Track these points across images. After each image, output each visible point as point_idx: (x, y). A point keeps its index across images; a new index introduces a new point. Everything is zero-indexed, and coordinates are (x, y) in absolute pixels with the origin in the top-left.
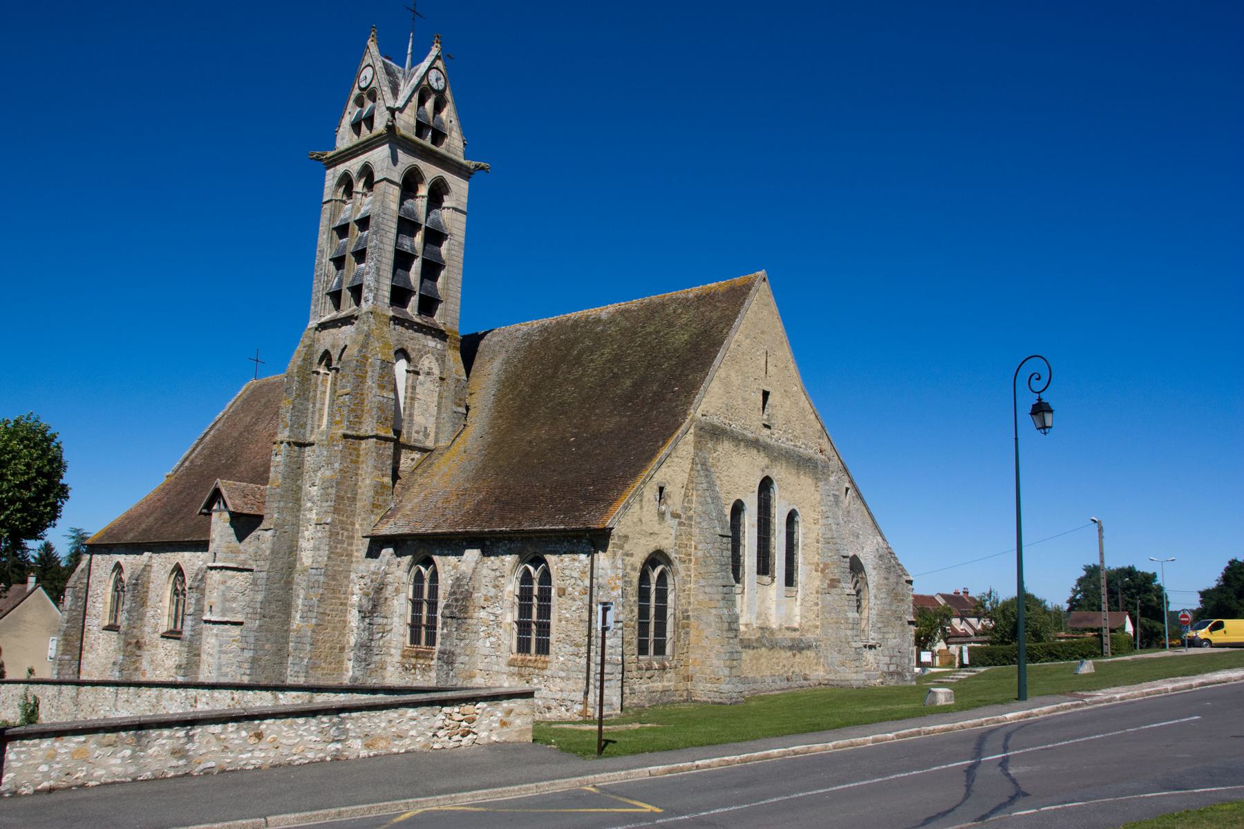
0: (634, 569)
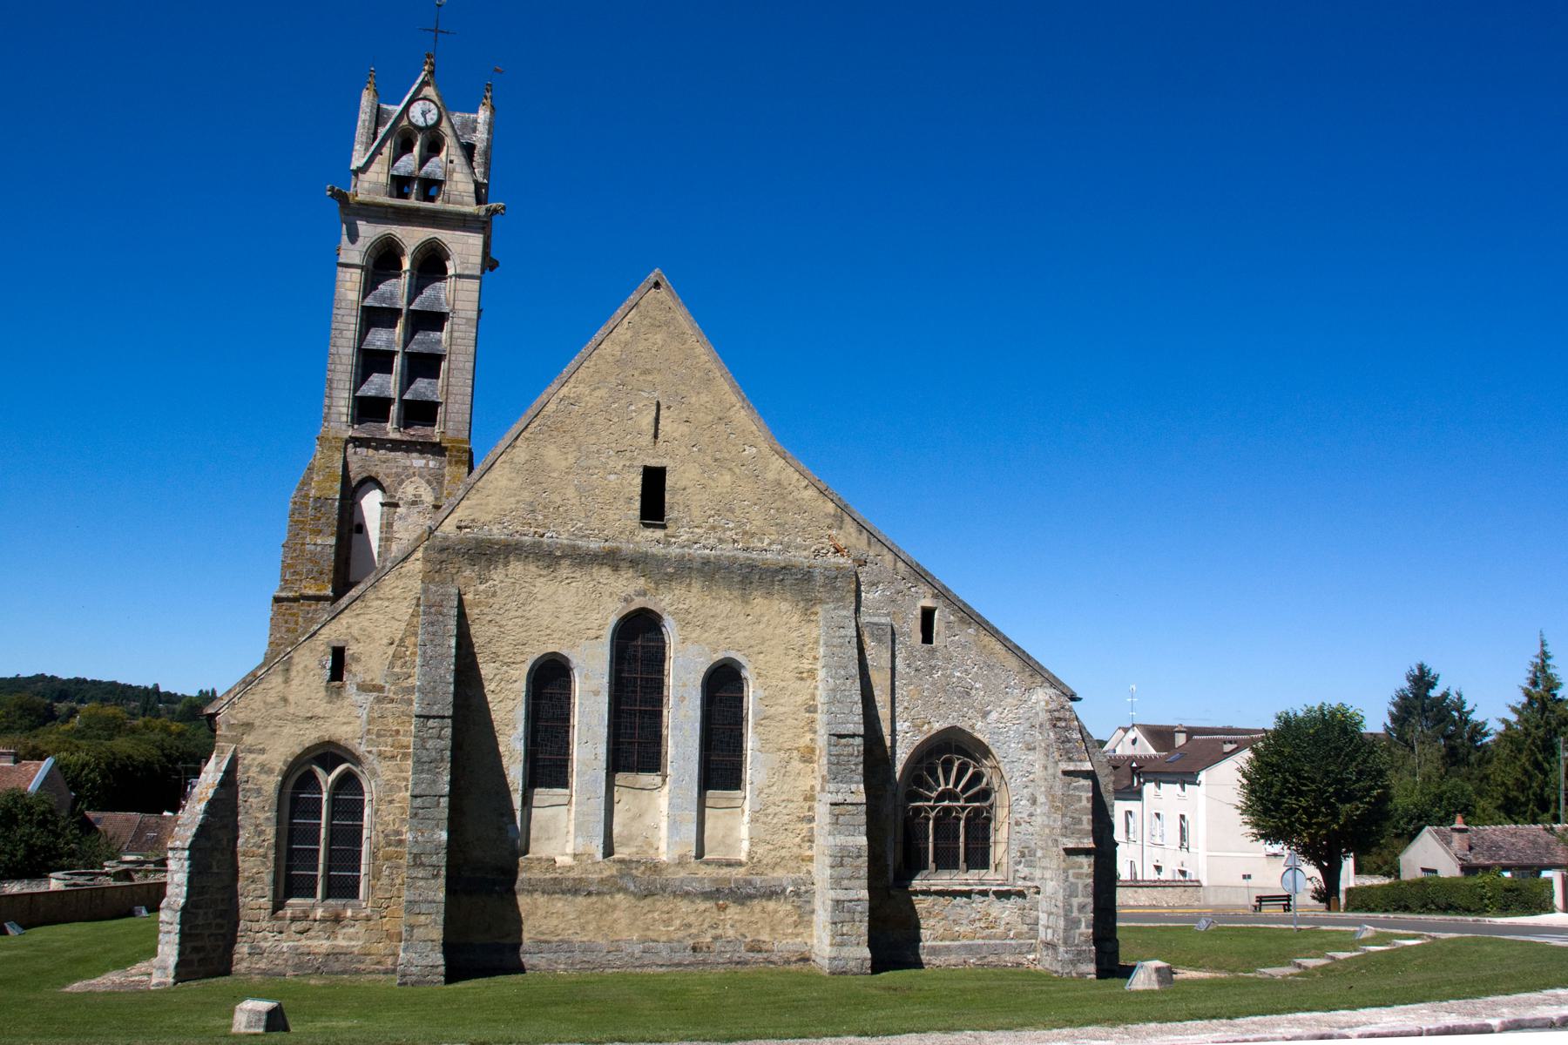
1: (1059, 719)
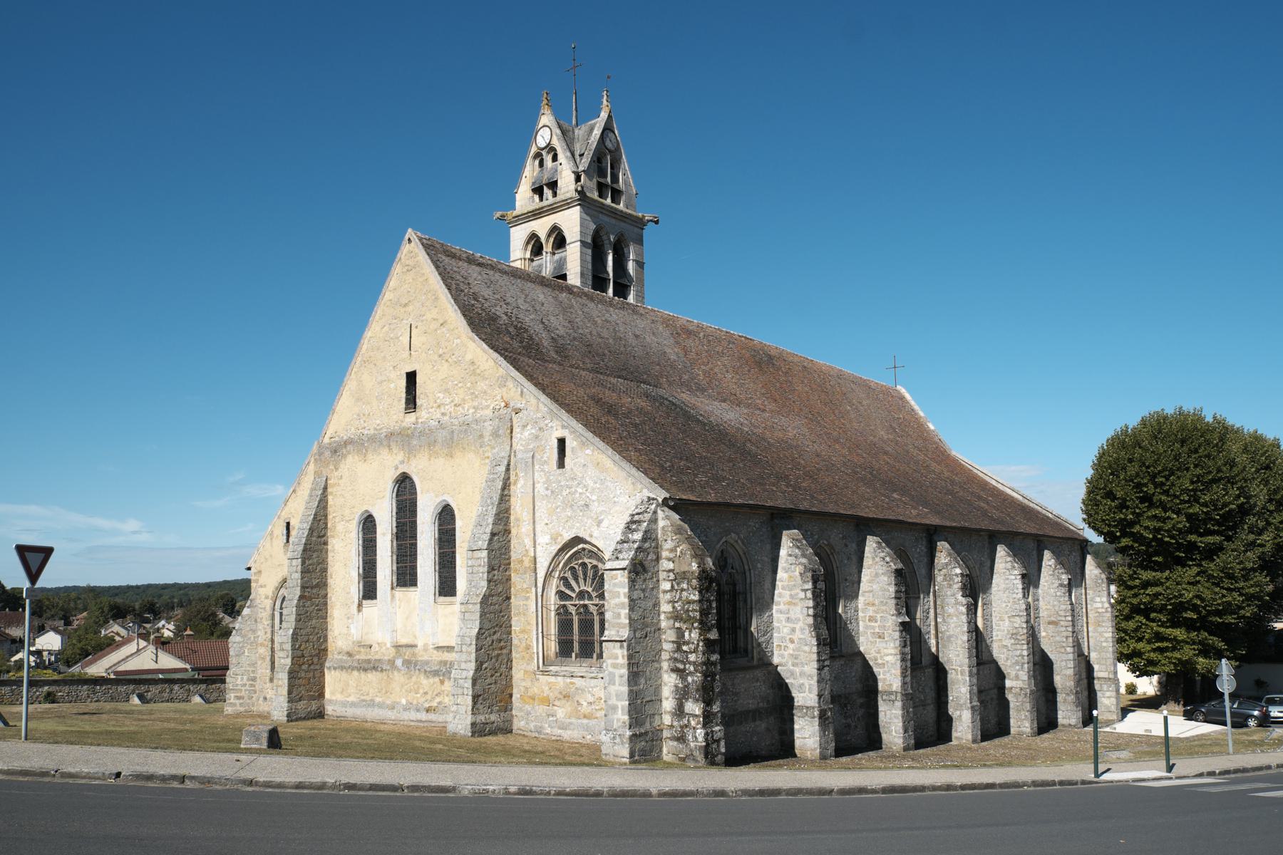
0: (267, 597)
1: (635, 522)
